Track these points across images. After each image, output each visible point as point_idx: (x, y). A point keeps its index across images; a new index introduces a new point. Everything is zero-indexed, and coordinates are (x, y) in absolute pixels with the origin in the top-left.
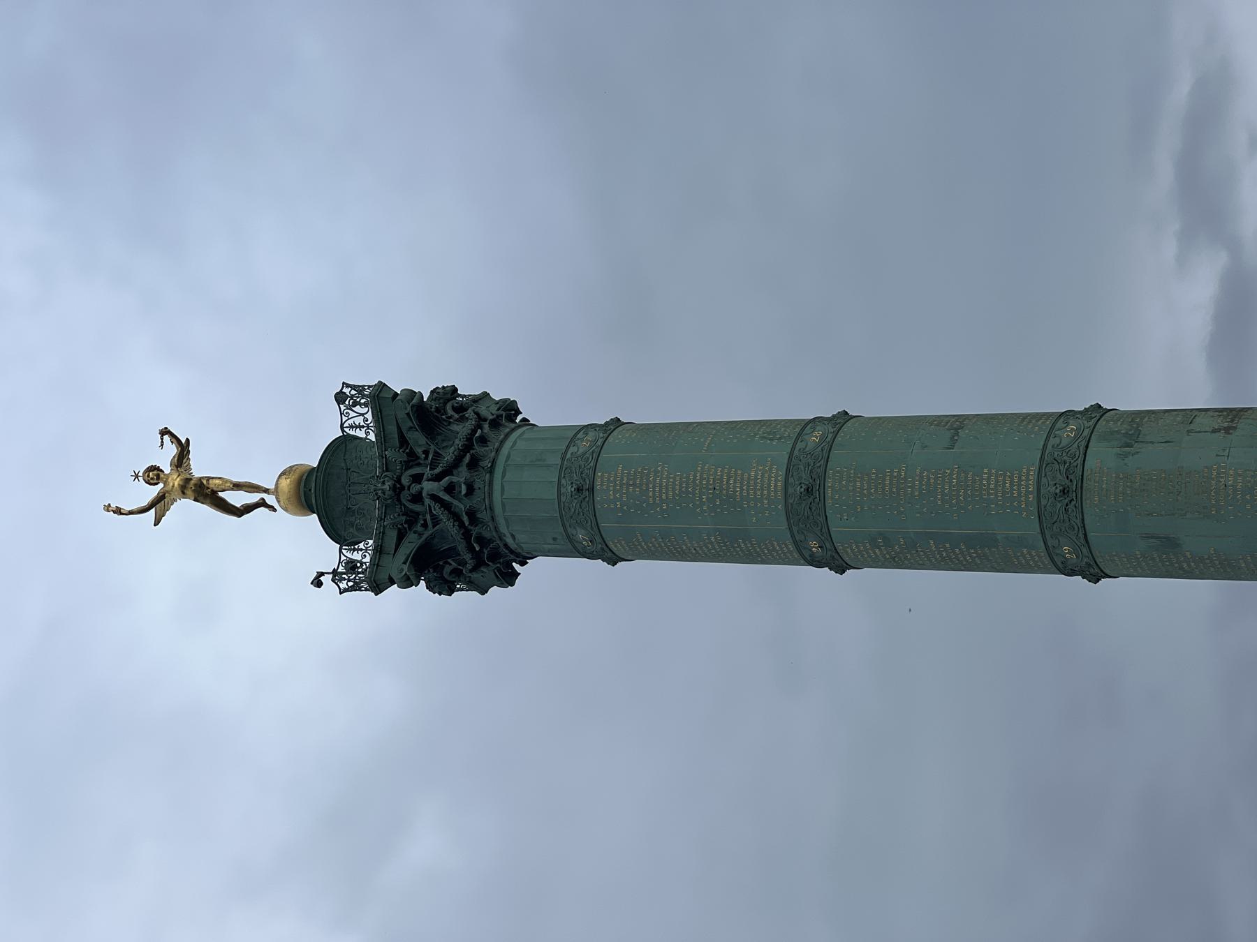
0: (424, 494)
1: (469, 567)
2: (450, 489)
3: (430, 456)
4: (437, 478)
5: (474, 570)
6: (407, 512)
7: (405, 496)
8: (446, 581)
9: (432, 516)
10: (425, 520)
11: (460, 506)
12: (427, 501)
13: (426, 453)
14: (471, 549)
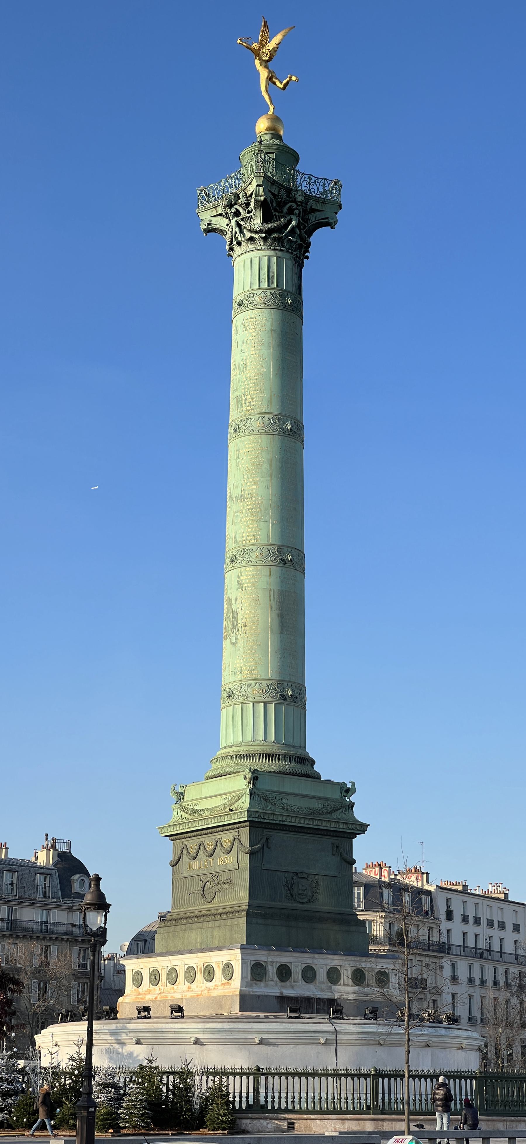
0: (292, 216)
1: (242, 223)
2: (292, 232)
5: (239, 225)
6: (285, 203)
7: (295, 206)
14: (261, 232)
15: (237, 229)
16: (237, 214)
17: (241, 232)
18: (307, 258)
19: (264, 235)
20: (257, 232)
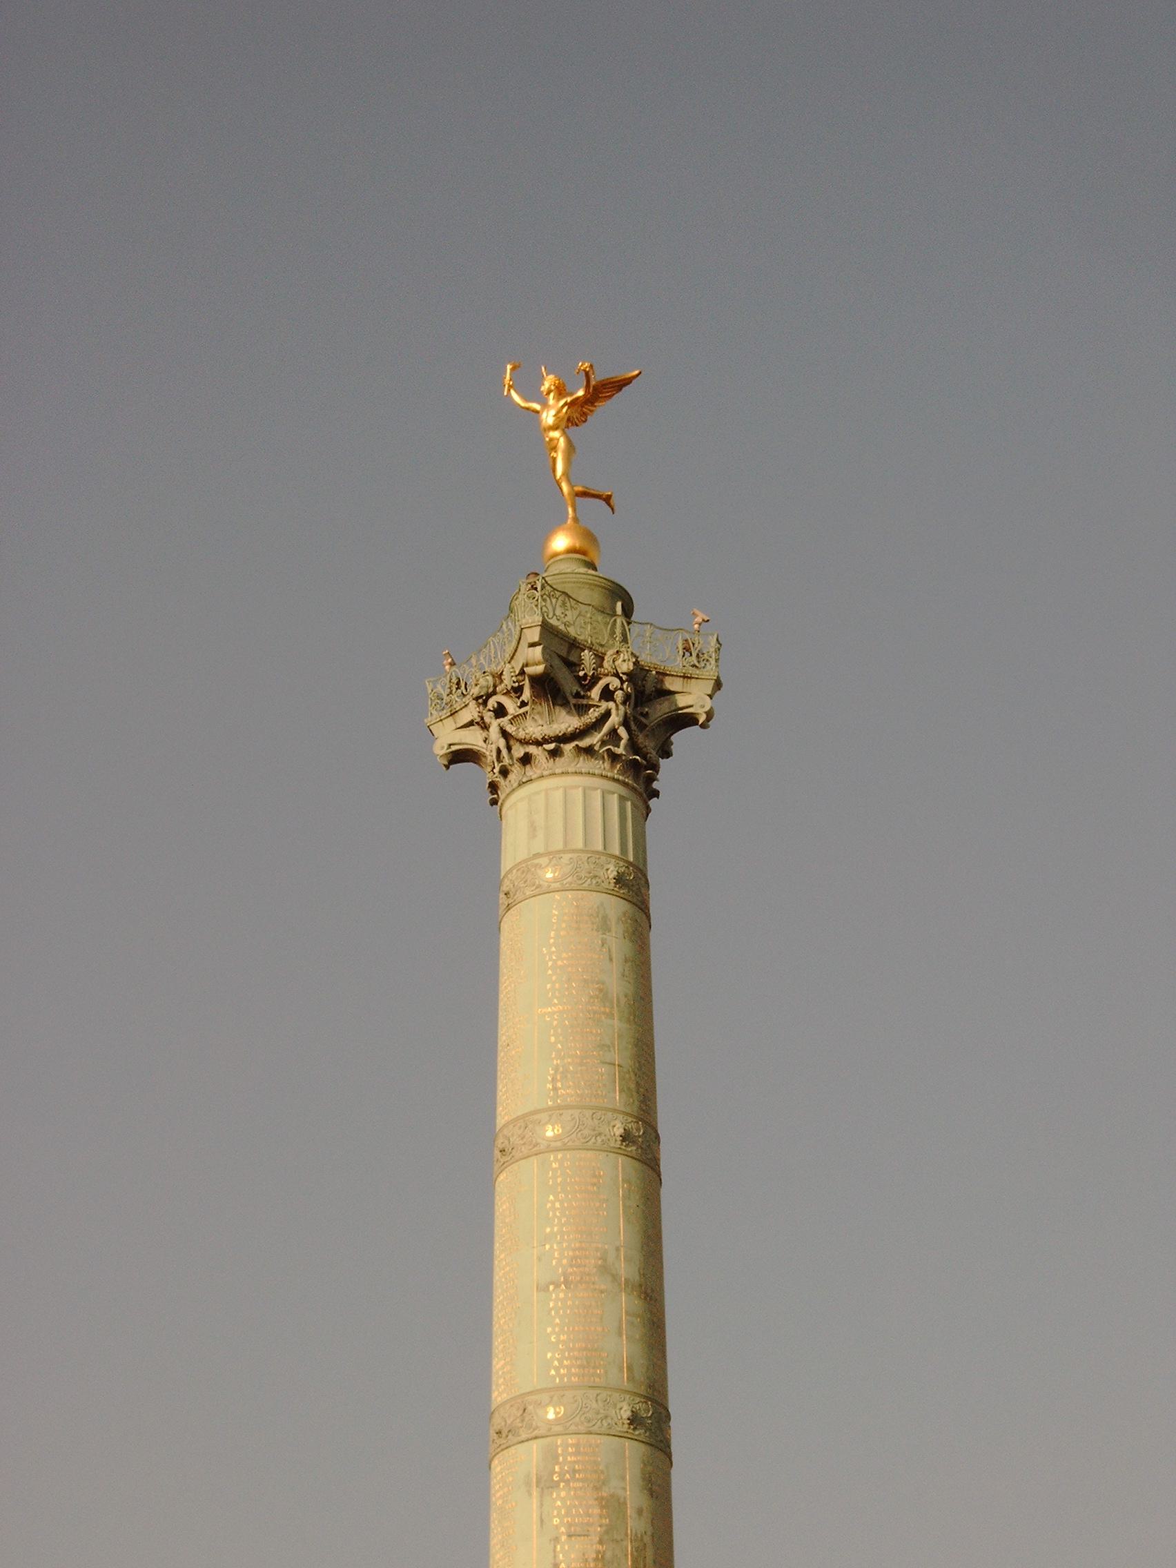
0: (611, 705)
1: (510, 729)
2: (613, 735)
3: (643, 719)
4: (625, 723)
5: (504, 734)
6: (595, 679)
7: (615, 683)
8: (489, 696)
9: (589, 707)
10: (583, 697)
11: (594, 739)
12: (605, 705)
13: (646, 715)
14: (546, 740)
15: (502, 743)
16: (500, 711)
17: (509, 748)
18: (656, 794)
19: (552, 746)
20: (538, 743)
